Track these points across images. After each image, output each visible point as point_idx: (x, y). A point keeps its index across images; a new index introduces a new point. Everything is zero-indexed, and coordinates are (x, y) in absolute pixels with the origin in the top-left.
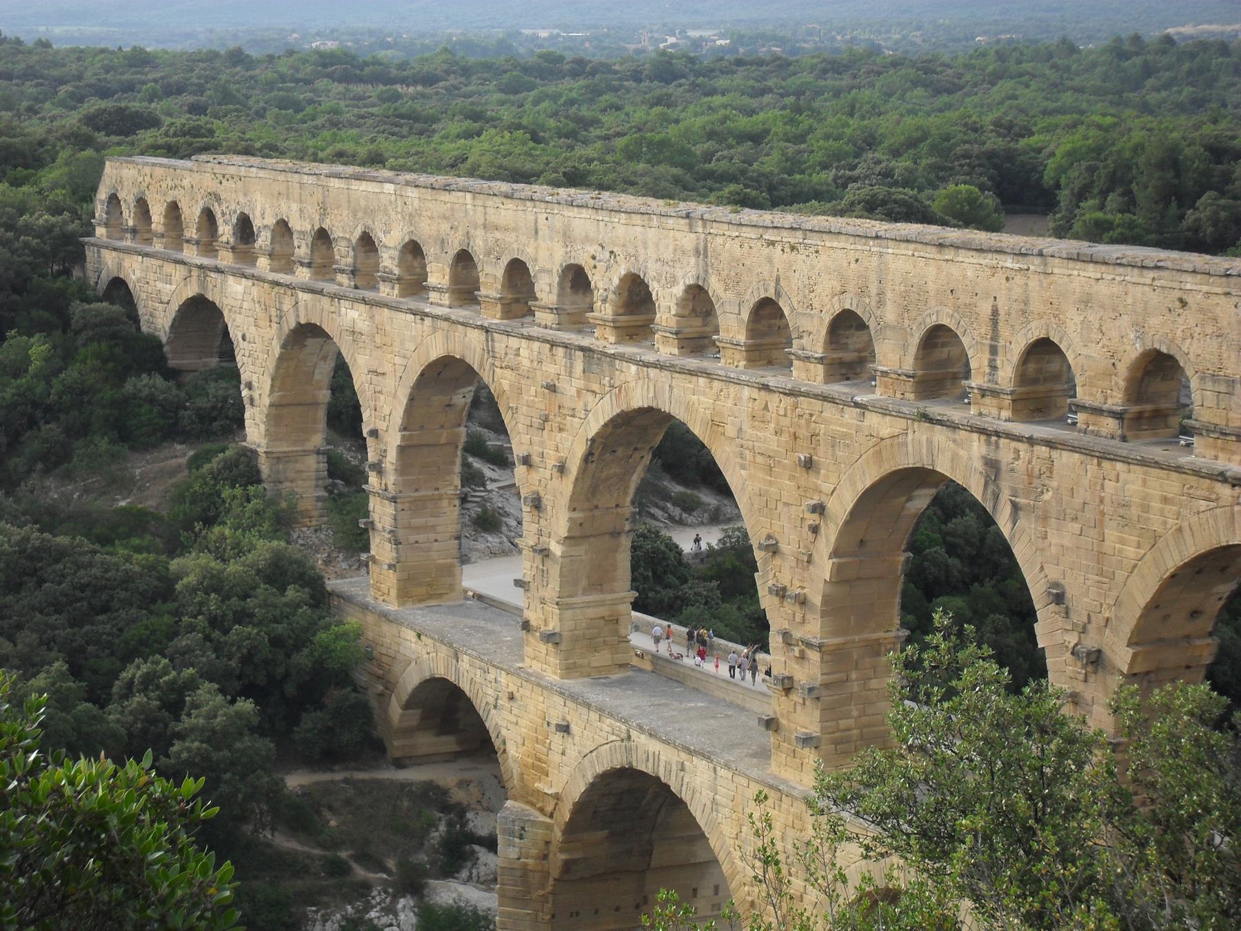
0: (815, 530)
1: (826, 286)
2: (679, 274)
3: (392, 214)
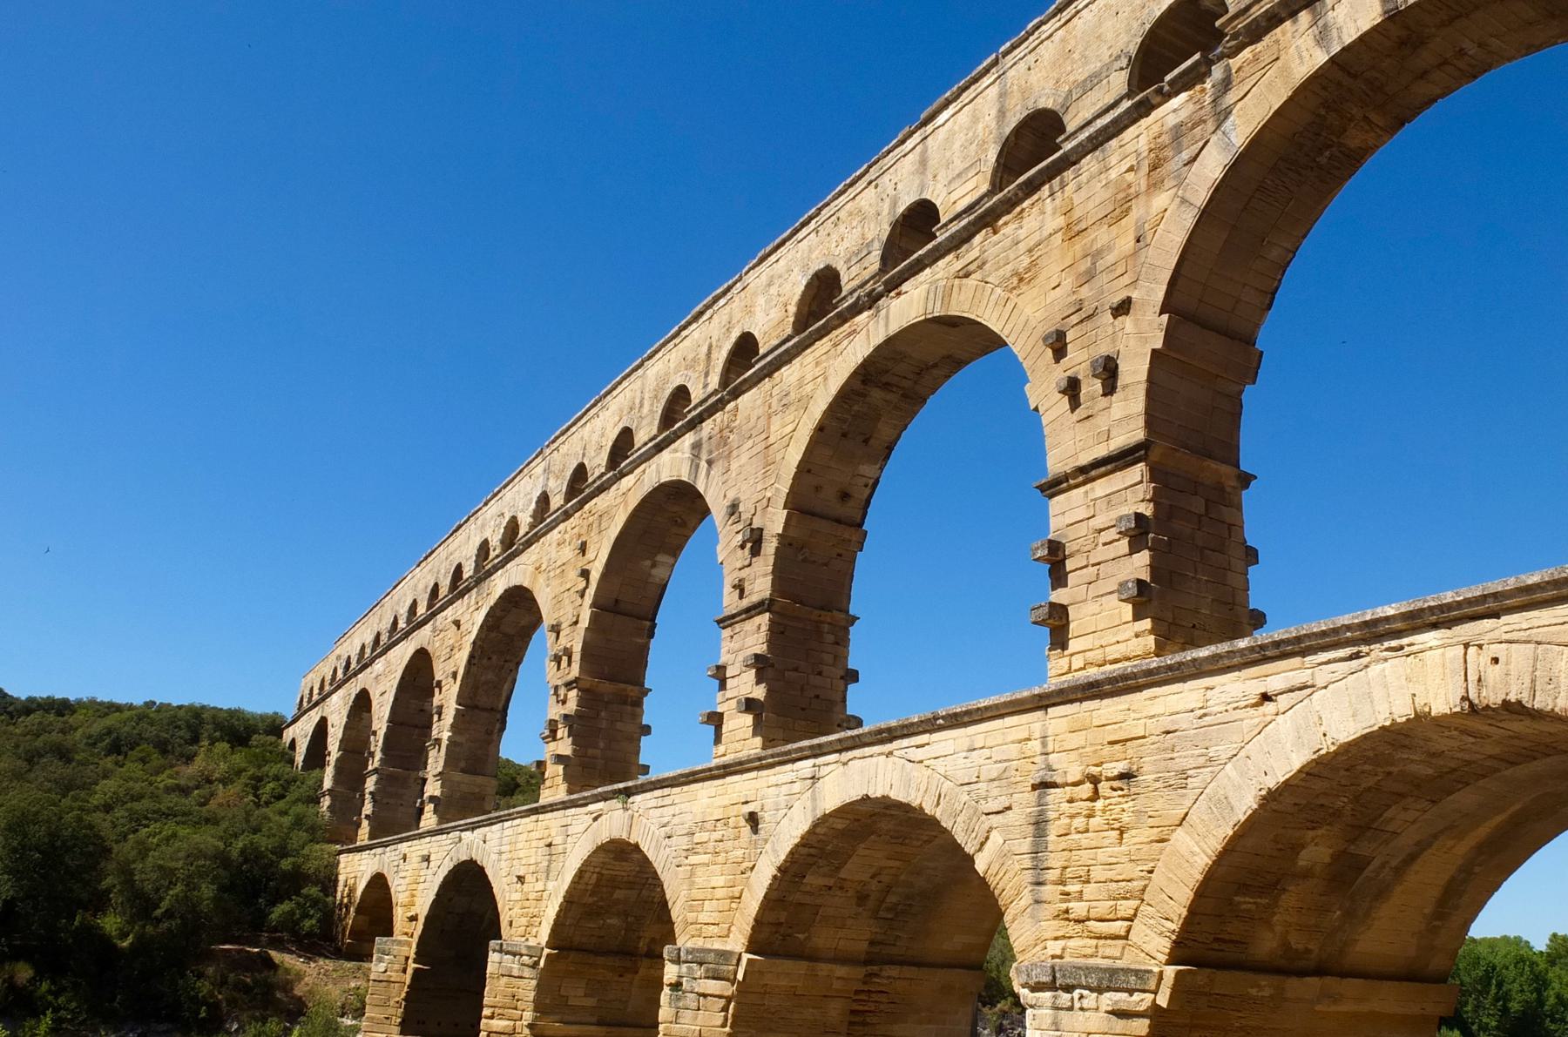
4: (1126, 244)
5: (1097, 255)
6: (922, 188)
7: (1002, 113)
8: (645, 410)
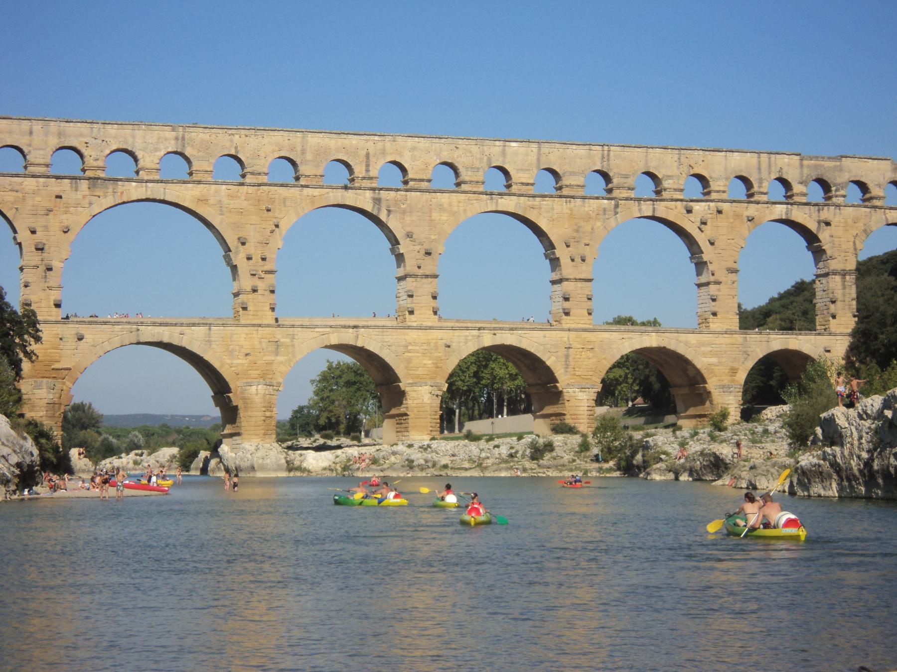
0: (272, 232)
2: (162, 146)
4: (588, 228)
5: (579, 227)
6: (504, 162)
7: (538, 160)
8: (309, 156)
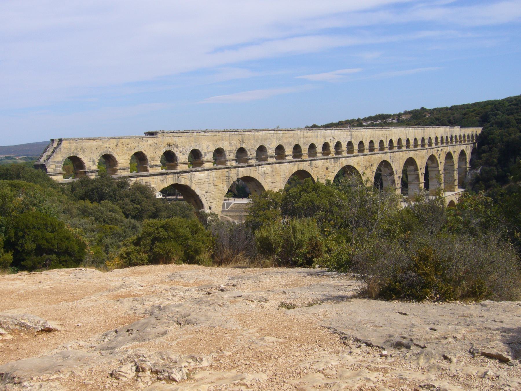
1: (369, 136)
3: (273, 139)
